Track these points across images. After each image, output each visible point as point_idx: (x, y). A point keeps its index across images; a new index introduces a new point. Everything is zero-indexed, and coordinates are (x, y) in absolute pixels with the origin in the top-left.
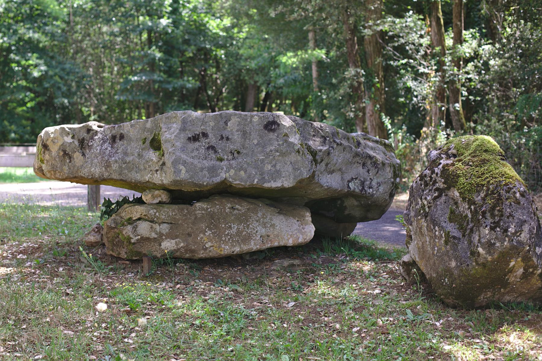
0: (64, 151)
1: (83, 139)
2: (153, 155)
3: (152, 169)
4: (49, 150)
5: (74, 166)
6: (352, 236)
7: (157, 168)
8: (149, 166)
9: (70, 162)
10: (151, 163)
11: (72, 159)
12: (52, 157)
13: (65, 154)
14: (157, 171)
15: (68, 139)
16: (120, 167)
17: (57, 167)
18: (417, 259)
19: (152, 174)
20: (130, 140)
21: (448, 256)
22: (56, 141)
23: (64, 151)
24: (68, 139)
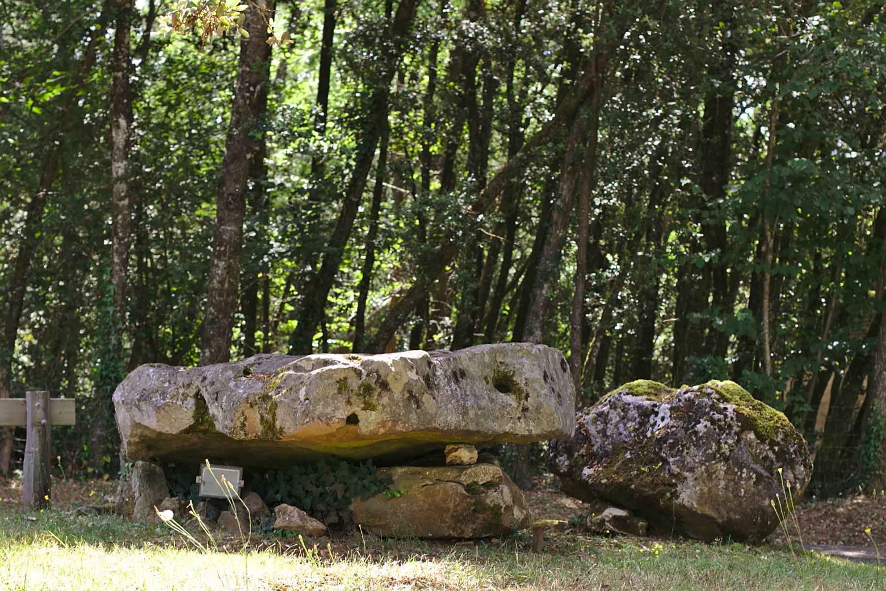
0: (410, 392)
1: (428, 375)
2: (510, 399)
3: (513, 416)
4: (389, 390)
5: (427, 413)
6: (200, 495)
7: (519, 415)
8: (508, 413)
9: (418, 407)
10: (509, 409)
11: (420, 403)
12: (393, 400)
13: (412, 396)
14: (519, 418)
15: (413, 375)
16: (476, 414)
17: (399, 415)
18: (695, 506)
19: (514, 423)
20: (473, 378)
21: (760, 496)
22: (399, 377)
23: (410, 392)
24: (413, 375)
